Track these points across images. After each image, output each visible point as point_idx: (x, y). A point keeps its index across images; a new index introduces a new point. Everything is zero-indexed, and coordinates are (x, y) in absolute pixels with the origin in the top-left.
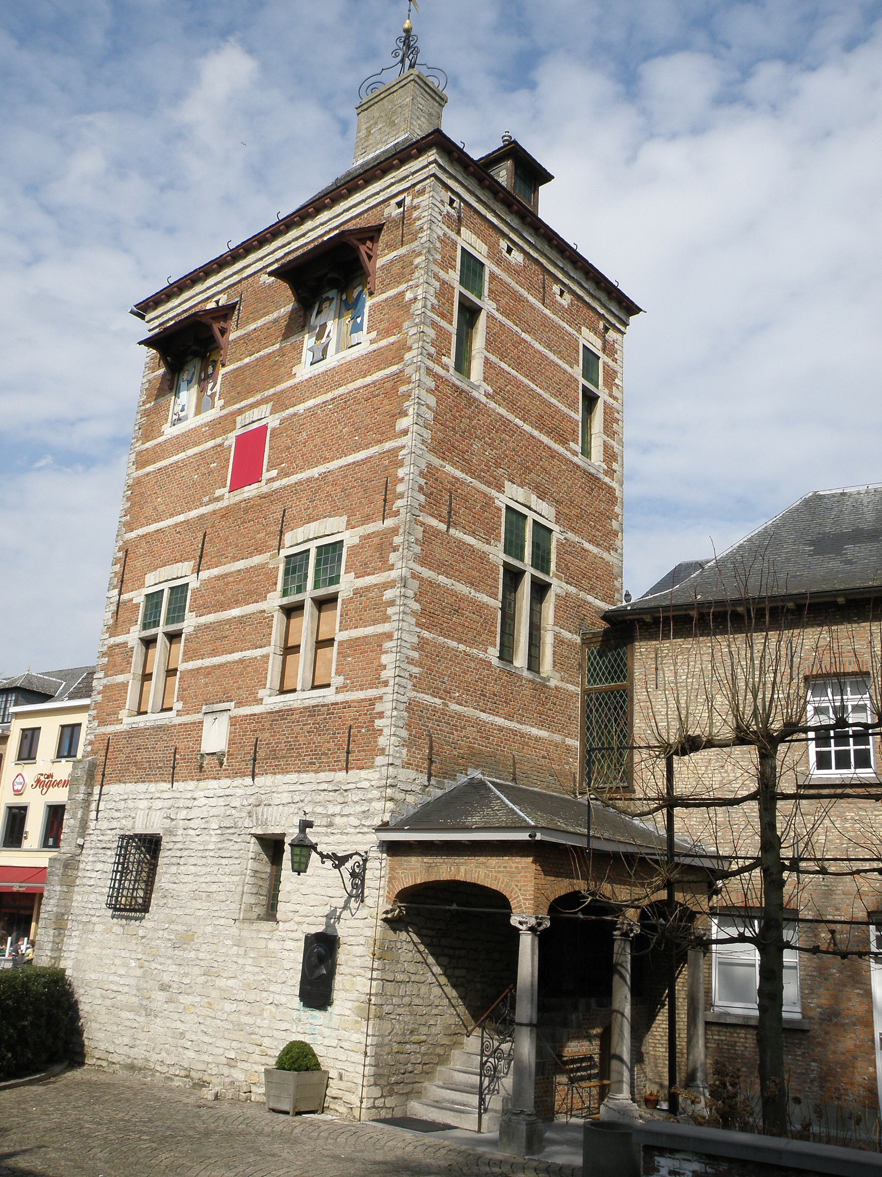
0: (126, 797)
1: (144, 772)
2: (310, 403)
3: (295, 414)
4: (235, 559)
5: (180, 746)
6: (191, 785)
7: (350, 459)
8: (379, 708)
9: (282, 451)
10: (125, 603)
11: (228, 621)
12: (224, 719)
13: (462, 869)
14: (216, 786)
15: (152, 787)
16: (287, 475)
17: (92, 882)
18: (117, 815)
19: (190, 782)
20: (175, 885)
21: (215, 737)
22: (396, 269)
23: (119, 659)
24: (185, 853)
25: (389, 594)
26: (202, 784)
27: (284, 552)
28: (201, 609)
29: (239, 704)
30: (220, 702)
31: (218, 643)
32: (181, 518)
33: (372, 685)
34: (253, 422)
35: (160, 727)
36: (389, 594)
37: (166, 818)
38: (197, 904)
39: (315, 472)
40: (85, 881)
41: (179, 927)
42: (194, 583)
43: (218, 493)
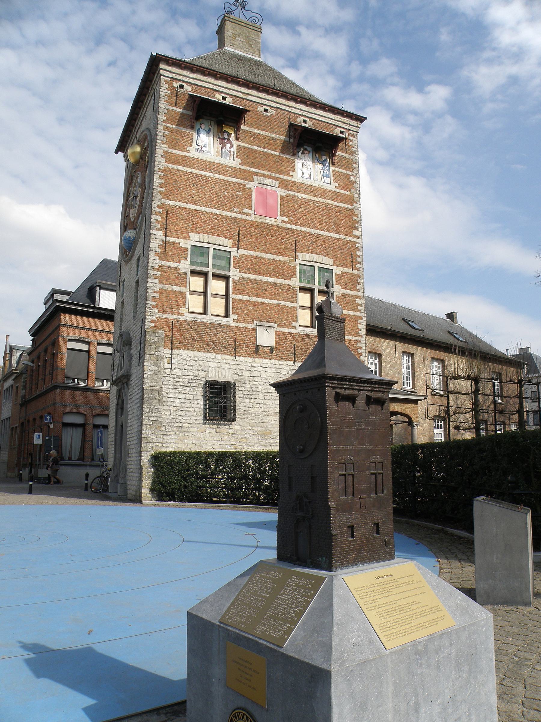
0: (197, 359)
1: (213, 347)
2: (304, 196)
3: (295, 196)
4: (264, 251)
5: (239, 338)
6: (250, 360)
7: (332, 235)
8: (359, 345)
9: (289, 211)
10: (172, 243)
11: (265, 282)
12: (272, 332)
13: (396, 407)
14: (269, 363)
15: (218, 356)
16: (294, 224)
17: (177, 404)
18: (188, 367)
19: (248, 358)
20: (250, 409)
21: (266, 338)
22: (345, 162)
23: (173, 277)
24: (254, 393)
25: (358, 301)
26: (257, 360)
27: (298, 262)
28: (243, 269)
29: (280, 326)
30: (267, 322)
31: (260, 292)
32: (217, 212)
33: (355, 335)
34: (265, 185)
35: (221, 325)
36: (358, 301)
37: (235, 374)
38: (270, 418)
39: (313, 231)
40: (169, 403)
41: (260, 429)
42: (234, 252)
43: (245, 210)
